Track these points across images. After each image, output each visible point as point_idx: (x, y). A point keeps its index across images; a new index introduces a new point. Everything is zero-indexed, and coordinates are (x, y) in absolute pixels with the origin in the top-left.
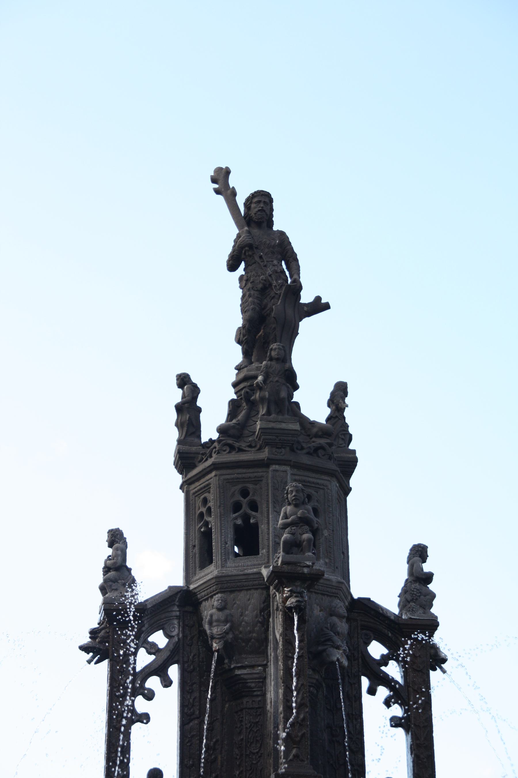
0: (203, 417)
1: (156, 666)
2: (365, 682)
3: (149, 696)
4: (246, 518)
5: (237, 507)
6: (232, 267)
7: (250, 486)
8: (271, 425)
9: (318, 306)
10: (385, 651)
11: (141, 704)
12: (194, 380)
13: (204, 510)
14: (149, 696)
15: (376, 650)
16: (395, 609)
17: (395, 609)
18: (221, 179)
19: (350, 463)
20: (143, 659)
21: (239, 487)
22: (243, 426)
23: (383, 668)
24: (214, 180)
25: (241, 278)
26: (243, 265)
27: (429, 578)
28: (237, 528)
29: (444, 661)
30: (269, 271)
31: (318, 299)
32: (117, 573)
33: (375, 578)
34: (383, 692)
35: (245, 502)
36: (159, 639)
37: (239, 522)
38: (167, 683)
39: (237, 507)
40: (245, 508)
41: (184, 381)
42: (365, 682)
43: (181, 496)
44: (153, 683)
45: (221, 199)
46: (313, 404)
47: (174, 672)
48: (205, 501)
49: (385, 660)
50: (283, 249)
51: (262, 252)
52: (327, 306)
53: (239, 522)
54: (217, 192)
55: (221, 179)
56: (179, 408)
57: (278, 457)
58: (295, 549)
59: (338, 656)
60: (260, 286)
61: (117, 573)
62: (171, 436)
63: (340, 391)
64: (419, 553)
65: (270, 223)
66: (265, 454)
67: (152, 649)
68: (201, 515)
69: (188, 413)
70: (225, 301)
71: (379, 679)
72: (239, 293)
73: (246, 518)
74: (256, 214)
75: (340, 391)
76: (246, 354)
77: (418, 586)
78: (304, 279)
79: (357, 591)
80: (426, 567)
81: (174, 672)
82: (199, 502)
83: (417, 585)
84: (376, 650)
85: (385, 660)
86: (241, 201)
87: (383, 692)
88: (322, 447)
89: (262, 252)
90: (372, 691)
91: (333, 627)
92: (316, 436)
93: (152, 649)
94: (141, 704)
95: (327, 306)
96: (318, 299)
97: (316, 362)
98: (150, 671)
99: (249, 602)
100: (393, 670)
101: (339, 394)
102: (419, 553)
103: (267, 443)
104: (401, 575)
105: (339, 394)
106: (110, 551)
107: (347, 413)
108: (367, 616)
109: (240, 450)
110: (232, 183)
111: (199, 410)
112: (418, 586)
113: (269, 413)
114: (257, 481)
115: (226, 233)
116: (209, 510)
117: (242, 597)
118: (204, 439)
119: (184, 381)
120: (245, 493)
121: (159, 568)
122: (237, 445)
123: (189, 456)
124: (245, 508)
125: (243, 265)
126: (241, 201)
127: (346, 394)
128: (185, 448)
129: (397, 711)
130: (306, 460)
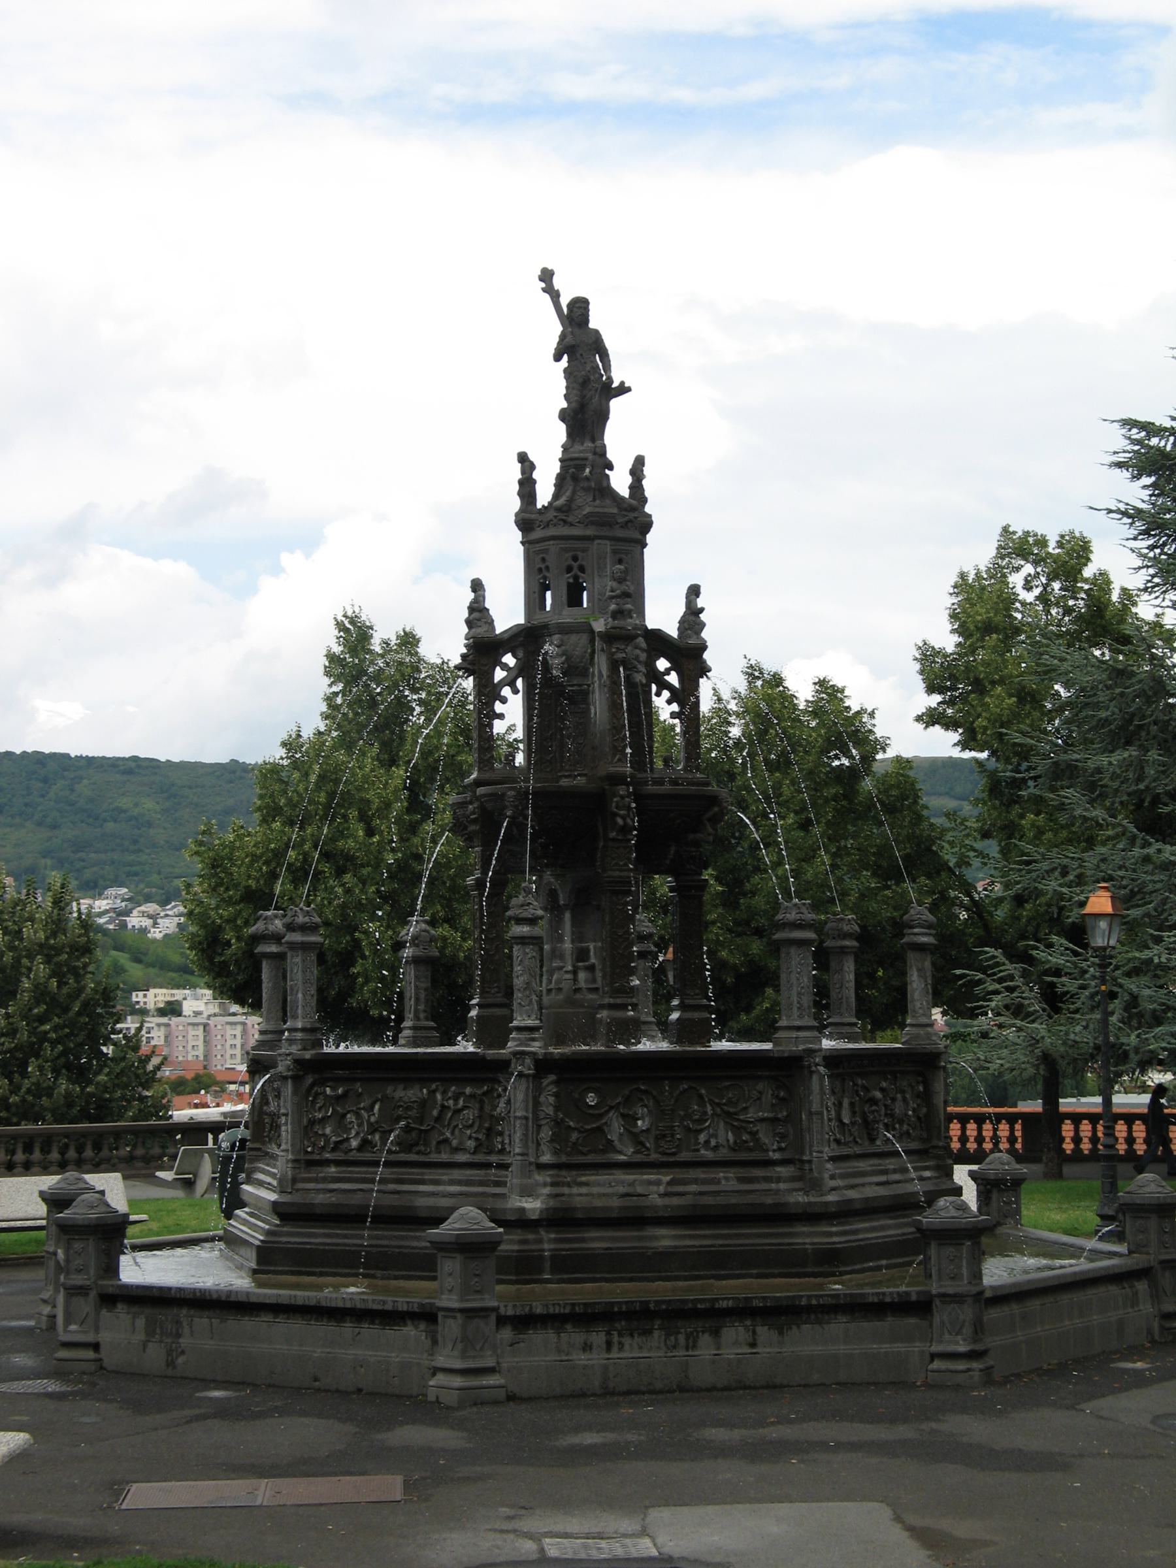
0: (537, 487)
1: (508, 680)
2: (654, 688)
3: (504, 701)
4: (576, 578)
5: (569, 569)
6: (558, 358)
7: (579, 554)
8: (597, 510)
9: (623, 390)
10: (668, 665)
11: (498, 707)
12: (531, 458)
13: (543, 566)
14: (504, 701)
15: (662, 664)
16: (674, 634)
17: (674, 634)
18: (547, 276)
19: (646, 525)
20: (499, 674)
21: (570, 554)
22: (571, 500)
23: (666, 677)
24: (541, 280)
25: (565, 371)
26: (565, 357)
27: (702, 610)
28: (569, 585)
29: (709, 670)
30: (588, 368)
31: (622, 383)
32: (478, 613)
33: (662, 613)
34: (666, 694)
35: (575, 565)
36: (509, 659)
37: (571, 580)
38: (515, 691)
39: (569, 569)
40: (575, 570)
41: (523, 458)
42: (654, 688)
43: (521, 549)
44: (506, 691)
45: (547, 296)
46: (620, 482)
47: (519, 683)
48: (543, 560)
49: (667, 672)
50: (597, 345)
51: (580, 345)
52: (629, 390)
53: (571, 580)
54: (544, 290)
55: (547, 276)
56: (521, 483)
57: (603, 534)
58: (619, 616)
59: (640, 678)
60: (581, 380)
61: (478, 613)
62: (516, 504)
63: (639, 462)
64: (694, 591)
65: (587, 321)
66: (589, 532)
67: (505, 667)
68: (540, 570)
69: (527, 487)
70: (551, 386)
71: (663, 685)
72: (564, 383)
73: (576, 578)
74: (576, 316)
75: (639, 462)
76: (570, 434)
77: (692, 618)
78: (613, 374)
79: (651, 623)
80: (700, 603)
81: (519, 683)
82: (538, 559)
83: (693, 618)
84: (662, 664)
85: (667, 672)
86: (564, 302)
87: (666, 694)
88: (630, 521)
89: (580, 345)
90: (658, 694)
91: (637, 658)
92: (626, 510)
93: (505, 667)
94: (498, 707)
95: (629, 390)
96: (622, 383)
97: (622, 437)
98: (503, 683)
99: (579, 642)
100: (673, 679)
101: (637, 469)
102: (694, 591)
103: (592, 523)
104: (681, 609)
105: (637, 469)
106: (472, 596)
107: (644, 482)
108: (658, 642)
109: (572, 525)
110: (557, 283)
111: (535, 482)
112: (692, 618)
113: (594, 500)
114: (584, 550)
115: (554, 329)
116: (547, 568)
117: (574, 638)
118: (539, 506)
119: (523, 458)
120: (575, 559)
121: (508, 611)
122: (570, 519)
123: (529, 521)
124: (575, 570)
125: (565, 357)
126: (564, 302)
127: (643, 465)
128: (527, 516)
129: (675, 707)
130: (620, 533)
